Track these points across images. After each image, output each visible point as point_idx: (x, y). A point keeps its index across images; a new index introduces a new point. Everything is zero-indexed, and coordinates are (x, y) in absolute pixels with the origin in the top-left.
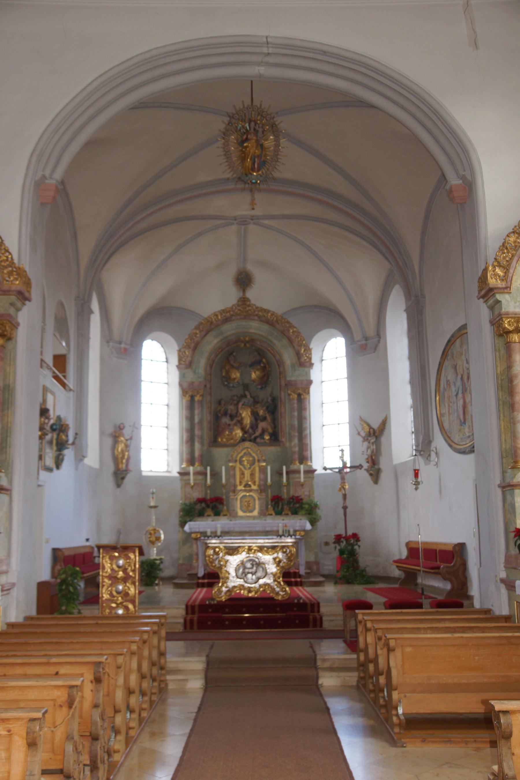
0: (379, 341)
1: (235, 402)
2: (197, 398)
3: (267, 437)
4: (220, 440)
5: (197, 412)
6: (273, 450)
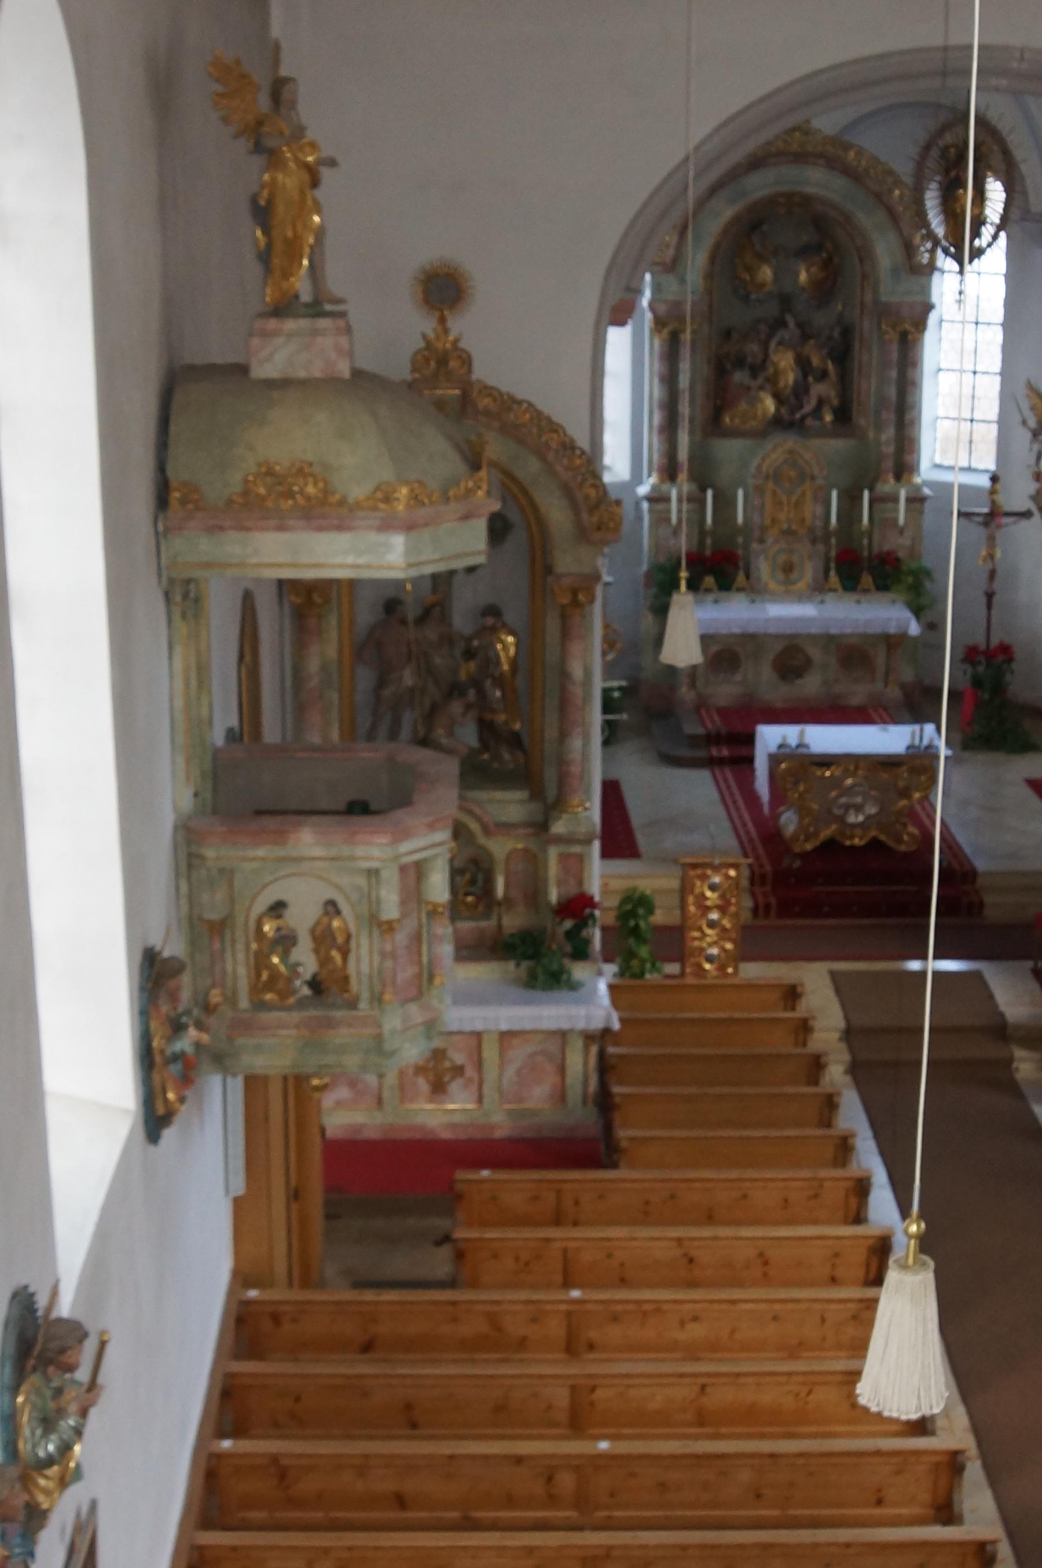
3: (828, 418)
4: (727, 420)
5: (685, 367)
6: (837, 446)
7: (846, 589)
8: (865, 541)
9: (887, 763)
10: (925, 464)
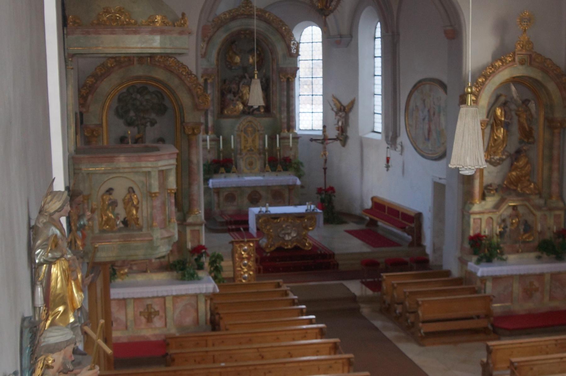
0: (351, 40)
1: (237, 82)
2: (209, 81)
3: (262, 110)
4: (226, 112)
6: (266, 121)
7: (272, 171)
8: (278, 153)
9: (300, 216)
10: (297, 128)
